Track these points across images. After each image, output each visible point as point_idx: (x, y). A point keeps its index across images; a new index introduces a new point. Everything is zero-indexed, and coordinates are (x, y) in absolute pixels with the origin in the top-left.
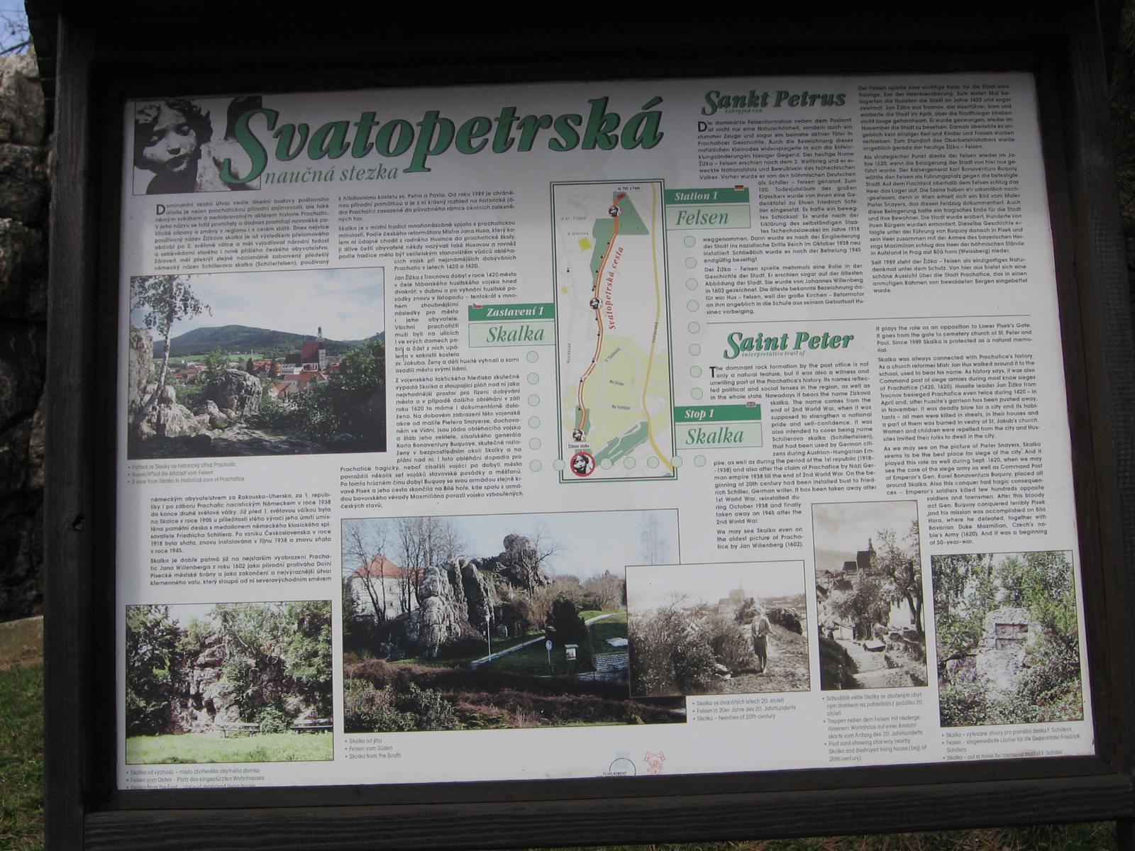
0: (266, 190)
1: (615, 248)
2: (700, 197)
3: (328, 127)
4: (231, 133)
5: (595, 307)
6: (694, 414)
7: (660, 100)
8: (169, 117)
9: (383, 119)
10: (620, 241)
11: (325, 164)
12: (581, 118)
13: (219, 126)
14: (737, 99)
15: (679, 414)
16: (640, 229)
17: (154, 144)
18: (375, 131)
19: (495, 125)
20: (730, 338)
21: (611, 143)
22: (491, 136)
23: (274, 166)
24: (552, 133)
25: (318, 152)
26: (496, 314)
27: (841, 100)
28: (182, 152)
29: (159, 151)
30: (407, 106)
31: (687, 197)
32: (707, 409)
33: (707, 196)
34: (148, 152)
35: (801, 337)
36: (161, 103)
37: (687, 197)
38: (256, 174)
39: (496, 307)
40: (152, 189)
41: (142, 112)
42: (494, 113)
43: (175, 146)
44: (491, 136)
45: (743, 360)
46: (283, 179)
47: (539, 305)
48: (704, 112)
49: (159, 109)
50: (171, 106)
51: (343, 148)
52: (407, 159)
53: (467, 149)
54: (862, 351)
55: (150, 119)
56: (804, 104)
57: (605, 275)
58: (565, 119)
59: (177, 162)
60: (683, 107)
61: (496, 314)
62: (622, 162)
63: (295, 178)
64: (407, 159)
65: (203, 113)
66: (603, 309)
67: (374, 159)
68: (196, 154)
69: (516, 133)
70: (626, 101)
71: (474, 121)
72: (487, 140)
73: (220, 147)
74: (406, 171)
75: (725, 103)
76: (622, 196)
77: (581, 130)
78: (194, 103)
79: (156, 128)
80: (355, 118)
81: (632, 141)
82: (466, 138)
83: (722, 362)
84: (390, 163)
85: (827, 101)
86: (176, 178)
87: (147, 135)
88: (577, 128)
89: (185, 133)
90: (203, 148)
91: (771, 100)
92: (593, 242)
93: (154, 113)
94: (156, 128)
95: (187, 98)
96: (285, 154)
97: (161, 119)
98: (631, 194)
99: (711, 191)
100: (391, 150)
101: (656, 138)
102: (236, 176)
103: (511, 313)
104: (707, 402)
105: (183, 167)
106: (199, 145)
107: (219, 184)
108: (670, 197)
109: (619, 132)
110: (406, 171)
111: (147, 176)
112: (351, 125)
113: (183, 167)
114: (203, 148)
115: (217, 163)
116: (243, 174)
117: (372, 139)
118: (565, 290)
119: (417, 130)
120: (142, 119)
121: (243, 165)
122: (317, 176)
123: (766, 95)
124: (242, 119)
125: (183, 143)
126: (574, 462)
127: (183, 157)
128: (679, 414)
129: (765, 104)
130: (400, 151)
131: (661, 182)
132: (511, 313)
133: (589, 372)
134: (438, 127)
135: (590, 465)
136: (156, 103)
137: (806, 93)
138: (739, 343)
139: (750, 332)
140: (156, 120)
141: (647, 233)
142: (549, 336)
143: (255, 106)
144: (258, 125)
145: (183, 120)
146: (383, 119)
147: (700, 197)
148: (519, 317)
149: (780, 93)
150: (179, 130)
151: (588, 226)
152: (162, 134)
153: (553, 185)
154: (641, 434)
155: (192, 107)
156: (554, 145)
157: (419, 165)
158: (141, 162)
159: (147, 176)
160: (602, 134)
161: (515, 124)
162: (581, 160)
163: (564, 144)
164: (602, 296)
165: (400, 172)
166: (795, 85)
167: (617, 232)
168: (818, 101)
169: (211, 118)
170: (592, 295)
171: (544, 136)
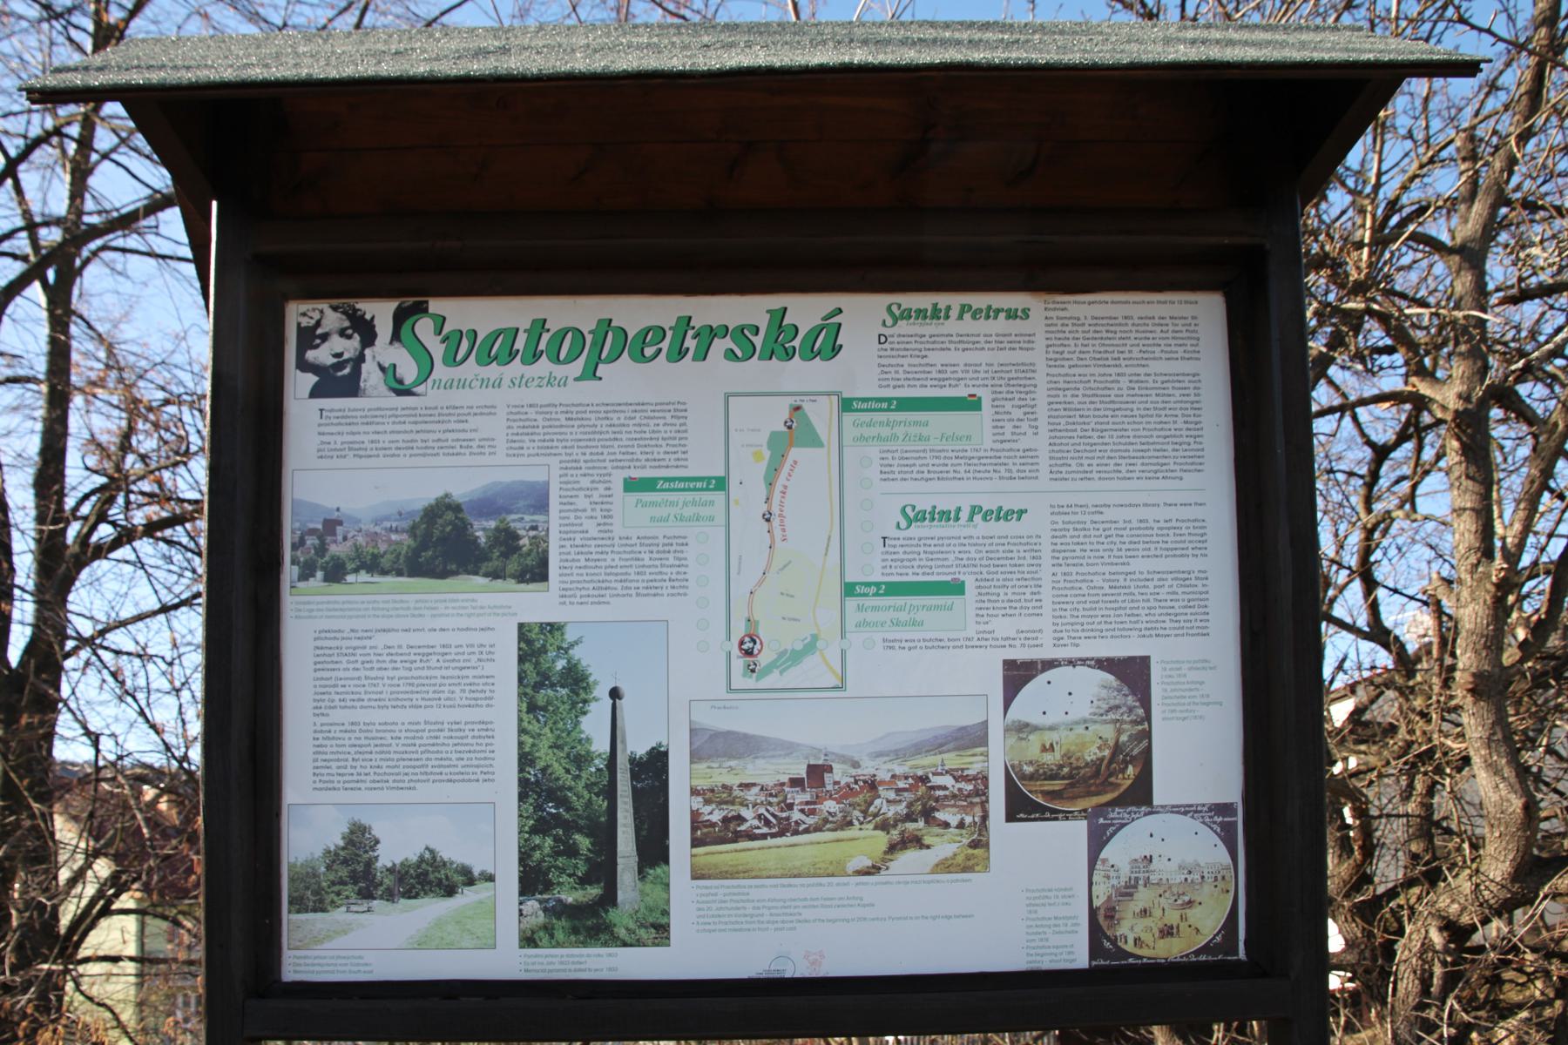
0: (430, 396)
1: (789, 461)
2: (878, 405)
3: (498, 333)
4: (396, 337)
5: (768, 520)
6: (864, 590)
7: (840, 311)
8: (333, 320)
9: (553, 326)
10: (795, 453)
11: (494, 370)
12: (758, 329)
13: (384, 328)
14: (919, 311)
15: (849, 590)
16: (815, 442)
17: (317, 346)
18: (546, 337)
19: (669, 334)
20: (903, 510)
21: (789, 355)
22: (665, 345)
23: (441, 372)
24: (727, 343)
25: (488, 358)
26: (666, 485)
27: (1026, 314)
28: (346, 356)
29: (322, 355)
30: (577, 312)
31: (864, 406)
32: (878, 584)
33: (885, 405)
34: (311, 355)
35: (975, 509)
36: (324, 305)
37: (864, 406)
38: (424, 377)
39: (666, 480)
40: (316, 393)
41: (304, 314)
42: (668, 322)
43: (339, 350)
44: (665, 345)
45: (916, 531)
46: (449, 385)
47: (710, 478)
48: (884, 323)
49: (322, 312)
50: (335, 309)
51: (512, 355)
52: (577, 367)
53: (641, 357)
54: (1038, 523)
55: (313, 322)
56: (988, 317)
57: (778, 488)
58: (742, 329)
59: (339, 366)
60: (862, 314)
61: (666, 485)
62: (800, 374)
63: (462, 384)
64: (577, 367)
65: (368, 317)
66: (776, 522)
67: (544, 366)
68: (360, 359)
69: (690, 343)
70: (806, 310)
71: (649, 330)
72: (660, 350)
73: (384, 351)
74: (576, 379)
75: (906, 315)
76: (798, 408)
77: (758, 341)
78: (358, 306)
79: (319, 331)
80: (524, 324)
81: (812, 353)
82: (641, 346)
83: (892, 532)
84: (560, 371)
85: (1012, 315)
86: (339, 382)
87: (309, 337)
88: (753, 339)
89: (349, 337)
90: (367, 352)
91: (954, 313)
92: (767, 454)
93: (317, 316)
94: (319, 331)
95: (351, 301)
96: (452, 360)
97: (324, 322)
98: (806, 406)
99: (889, 400)
100: (562, 357)
101: (836, 349)
102: (401, 382)
103: (681, 485)
104: (877, 577)
105: (347, 371)
106: (363, 348)
107: (383, 389)
108: (846, 405)
109: (796, 343)
110: (576, 379)
111: (312, 379)
112: (521, 333)
113: (347, 371)
114: (367, 352)
115: (382, 369)
116: (409, 380)
117: (542, 346)
118: (737, 502)
119: (589, 338)
120: (305, 322)
121: (408, 371)
122: (485, 383)
123: (949, 308)
124: (409, 322)
125: (350, 347)
126: (742, 643)
127: (347, 361)
128: (849, 590)
129: (947, 317)
130: (572, 359)
131: (838, 394)
132: (681, 485)
133: (760, 583)
134: (610, 335)
135: (758, 646)
136: (320, 306)
137: (990, 307)
138: (911, 515)
139: (924, 504)
140: (318, 324)
141: (821, 445)
142: (718, 510)
143: (421, 309)
144: (424, 327)
145: (347, 324)
146: (553, 326)
147: (878, 405)
148: (689, 490)
149: (963, 306)
150: (342, 333)
151: (763, 438)
152: (325, 337)
153: (728, 396)
154: (811, 646)
155: (355, 310)
156: (731, 355)
157: (591, 373)
158: (304, 366)
159: (312, 379)
160: (780, 342)
161: (690, 333)
162: (756, 371)
163: (739, 354)
164: (775, 510)
165: (570, 380)
166: (979, 300)
167: (791, 445)
168: (1002, 315)
169: (376, 322)
170: (764, 508)
171: (720, 345)
